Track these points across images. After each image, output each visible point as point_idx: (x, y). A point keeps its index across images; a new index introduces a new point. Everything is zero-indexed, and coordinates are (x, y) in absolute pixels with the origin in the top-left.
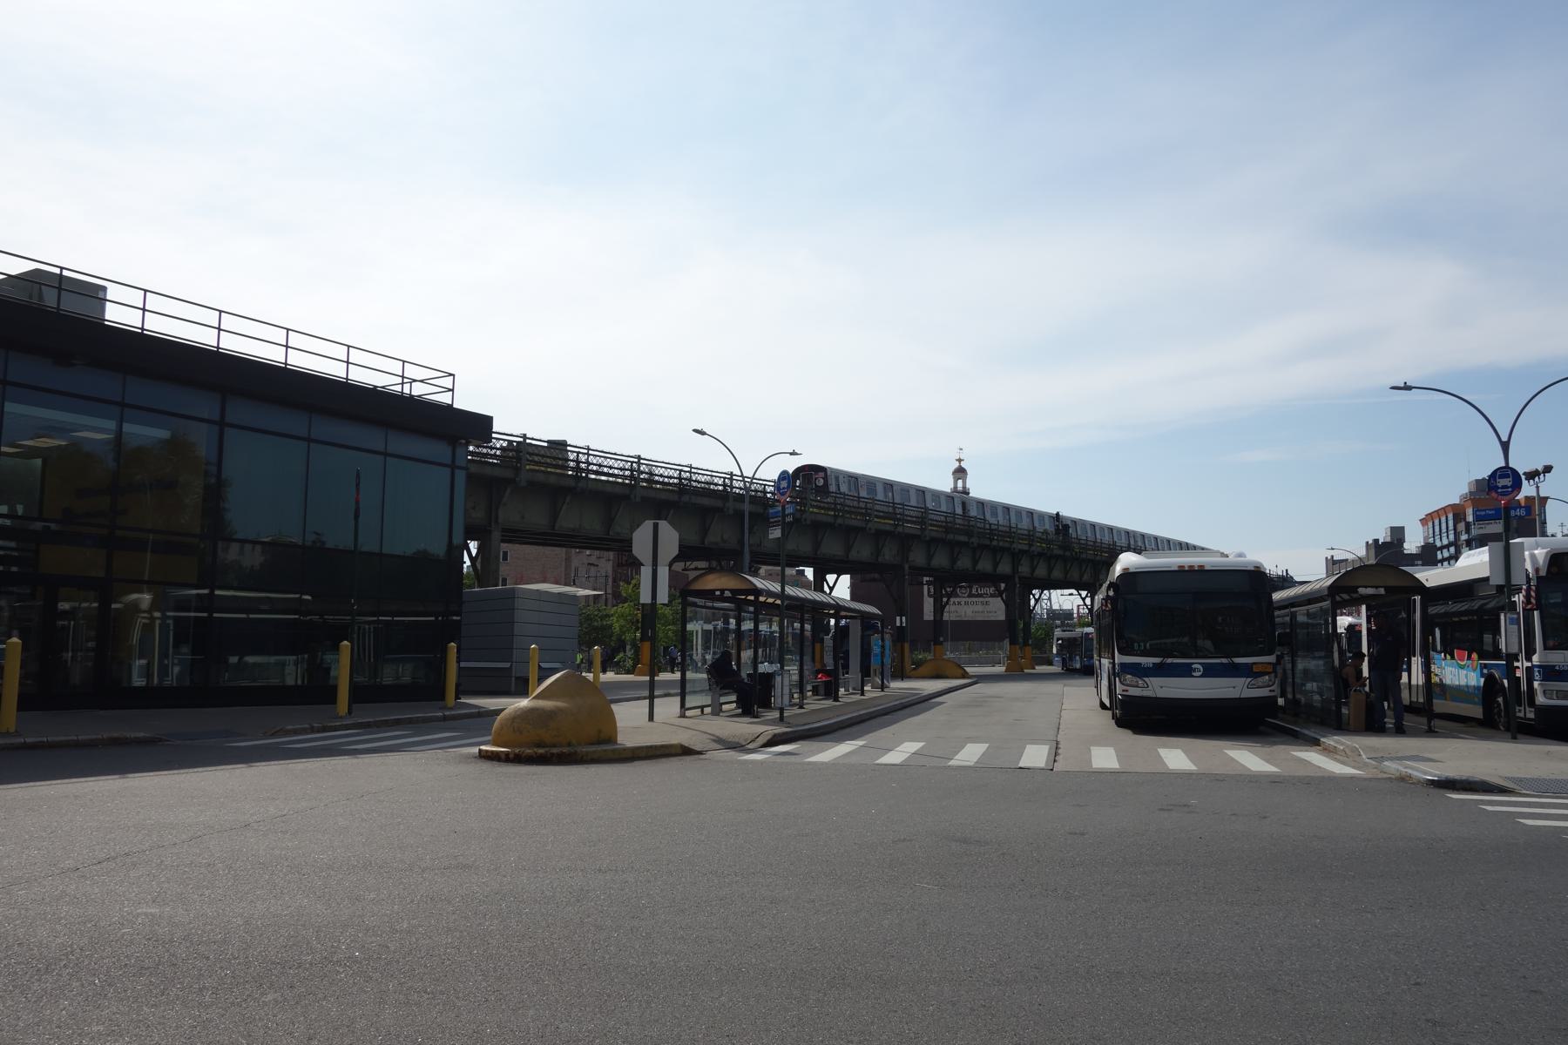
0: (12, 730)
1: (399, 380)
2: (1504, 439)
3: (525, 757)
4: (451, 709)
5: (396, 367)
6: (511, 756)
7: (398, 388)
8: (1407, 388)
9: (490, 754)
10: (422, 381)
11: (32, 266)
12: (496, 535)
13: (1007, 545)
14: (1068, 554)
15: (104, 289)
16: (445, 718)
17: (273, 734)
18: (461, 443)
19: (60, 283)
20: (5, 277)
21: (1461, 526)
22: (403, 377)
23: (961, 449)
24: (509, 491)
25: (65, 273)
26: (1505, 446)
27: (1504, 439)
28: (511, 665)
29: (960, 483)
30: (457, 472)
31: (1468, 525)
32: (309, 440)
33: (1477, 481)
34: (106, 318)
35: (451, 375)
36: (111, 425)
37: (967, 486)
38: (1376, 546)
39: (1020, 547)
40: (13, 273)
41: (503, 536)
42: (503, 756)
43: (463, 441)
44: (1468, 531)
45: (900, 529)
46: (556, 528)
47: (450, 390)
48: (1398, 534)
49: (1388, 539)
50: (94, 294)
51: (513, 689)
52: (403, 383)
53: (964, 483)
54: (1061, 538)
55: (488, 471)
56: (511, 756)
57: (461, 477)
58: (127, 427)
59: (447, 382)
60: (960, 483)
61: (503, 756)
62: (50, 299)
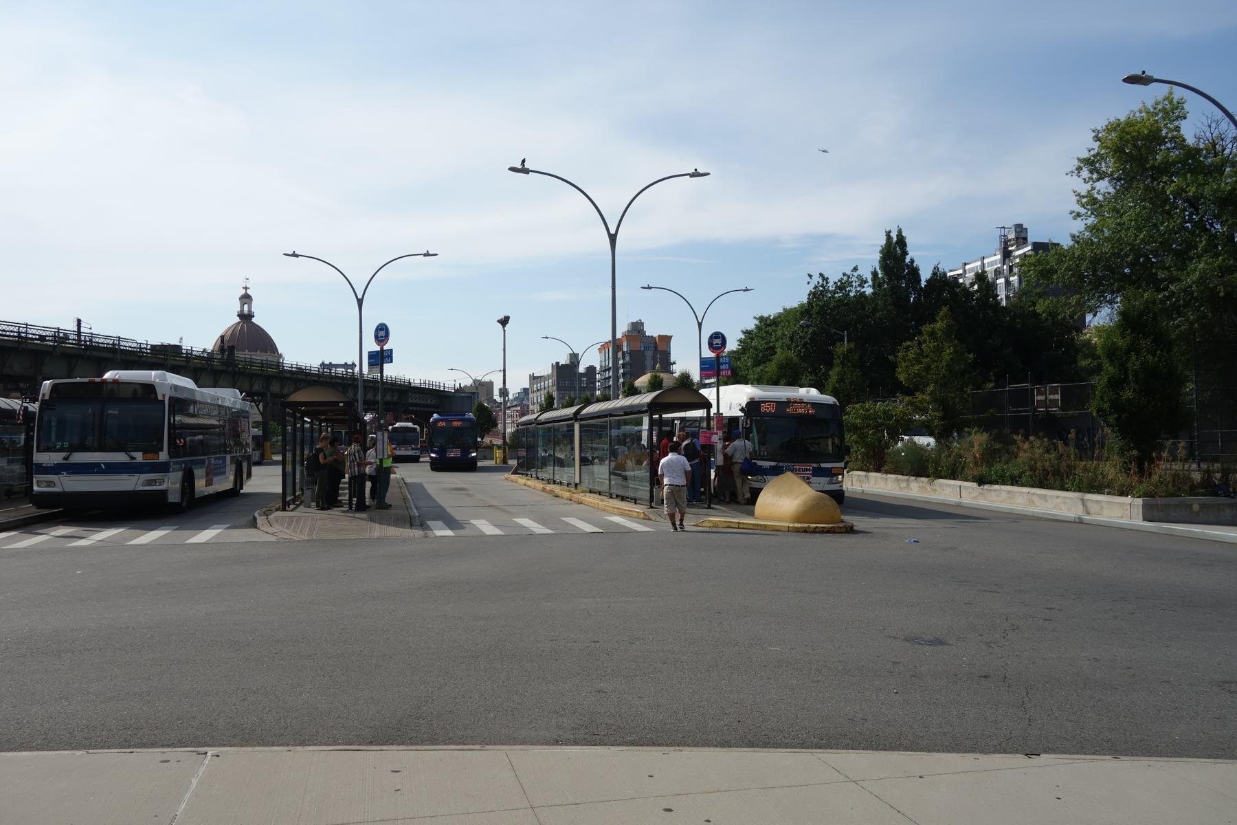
2: (360, 297)
8: (295, 255)
13: (159, 361)
14: (230, 369)
21: (620, 354)
23: (247, 279)
26: (360, 302)
27: (360, 297)
29: (246, 306)
31: (624, 353)
33: (632, 323)
37: (253, 310)
38: (558, 368)
39: (174, 363)
44: (623, 358)
45: (23, 346)
48: (575, 358)
49: (568, 362)
53: (250, 307)
54: (225, 357)
60: (246, 306)
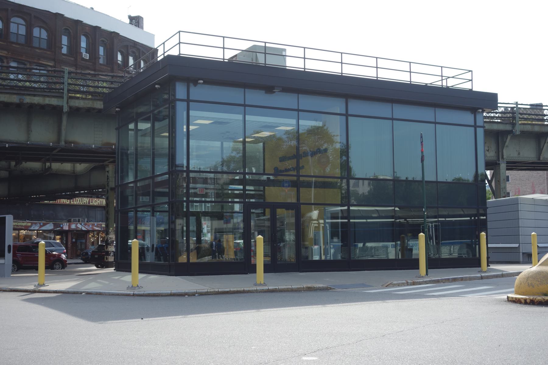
0: (262, 282)
1: (440, 78)
3: (537, 301)
4: (485, 272)
5: (438, 71)
6: (528, 301)
7: (440, 83)
9: (514, 299)
10: (453, 77)
11: (251, 44)
12: (503, 166)
15: (285, 50)
16: (482, 278)
17: (386, 286)
18: (479, 112)
19: (266, 51)
20: (241, 51)
22: (442, 76)
24: (509, 137)
25: (267, 45)
28: (519, 245)
30: (478, 129)
32: (392, 119)
34: (287, 65)
35: (470, 71)
36: (294, 122)
40: (244, 49)
41: (507, 166)
42: (523, 301)
43: (481, 110)
46: (541, 159)
47: (470, 80)
50: (280, 53)
51: (521, 260)
52: (442, 80)
55: (495, 127)
56: (528, 301)
57: (480, 132)
58: (301, 122)
59: (468, 76)
61: (523, 301)
62: (261, 60)
